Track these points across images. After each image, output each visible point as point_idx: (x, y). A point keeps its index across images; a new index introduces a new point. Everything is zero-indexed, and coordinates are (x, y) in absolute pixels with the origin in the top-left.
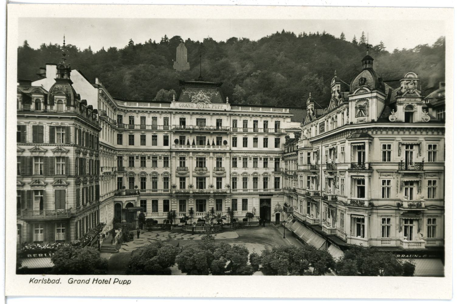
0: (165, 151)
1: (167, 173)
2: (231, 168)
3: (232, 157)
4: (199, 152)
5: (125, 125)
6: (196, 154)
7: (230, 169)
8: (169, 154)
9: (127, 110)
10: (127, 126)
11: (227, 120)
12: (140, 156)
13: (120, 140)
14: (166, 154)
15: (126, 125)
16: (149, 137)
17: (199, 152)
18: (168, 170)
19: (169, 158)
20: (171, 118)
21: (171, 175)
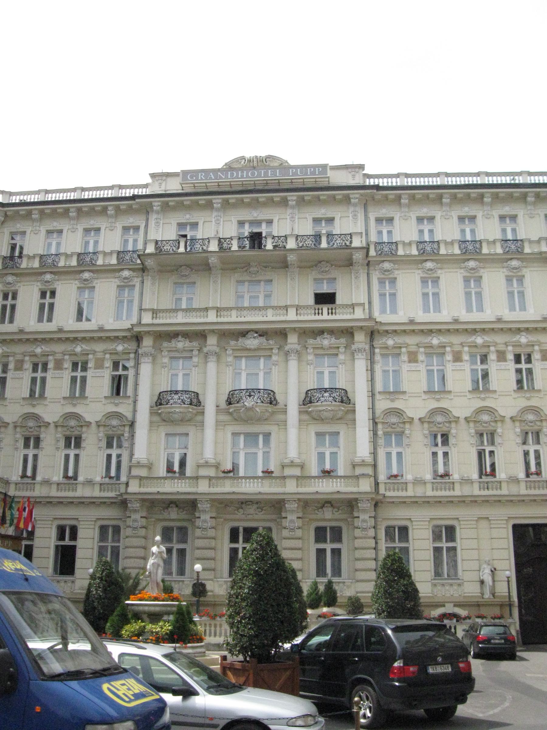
0: (117, 338)
1: (118, 415)
2: (378, 397)
3: (377, 351)
4: (244, 334)
6: (233, 343)
7: (373, 395)
8: (132, 346)
11: (355, 217)
14: (120, 348)
17: (244, 334)
18: (125, 409)
20: (146, 226)
21: (132, 424)
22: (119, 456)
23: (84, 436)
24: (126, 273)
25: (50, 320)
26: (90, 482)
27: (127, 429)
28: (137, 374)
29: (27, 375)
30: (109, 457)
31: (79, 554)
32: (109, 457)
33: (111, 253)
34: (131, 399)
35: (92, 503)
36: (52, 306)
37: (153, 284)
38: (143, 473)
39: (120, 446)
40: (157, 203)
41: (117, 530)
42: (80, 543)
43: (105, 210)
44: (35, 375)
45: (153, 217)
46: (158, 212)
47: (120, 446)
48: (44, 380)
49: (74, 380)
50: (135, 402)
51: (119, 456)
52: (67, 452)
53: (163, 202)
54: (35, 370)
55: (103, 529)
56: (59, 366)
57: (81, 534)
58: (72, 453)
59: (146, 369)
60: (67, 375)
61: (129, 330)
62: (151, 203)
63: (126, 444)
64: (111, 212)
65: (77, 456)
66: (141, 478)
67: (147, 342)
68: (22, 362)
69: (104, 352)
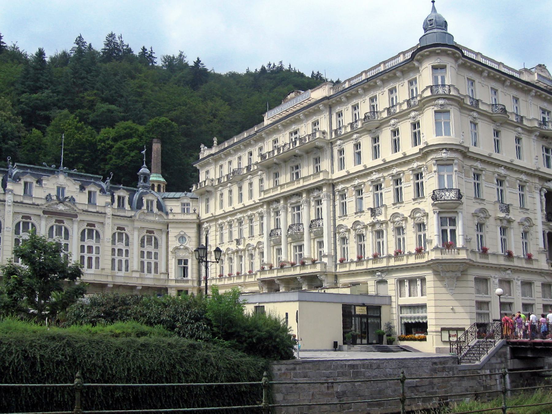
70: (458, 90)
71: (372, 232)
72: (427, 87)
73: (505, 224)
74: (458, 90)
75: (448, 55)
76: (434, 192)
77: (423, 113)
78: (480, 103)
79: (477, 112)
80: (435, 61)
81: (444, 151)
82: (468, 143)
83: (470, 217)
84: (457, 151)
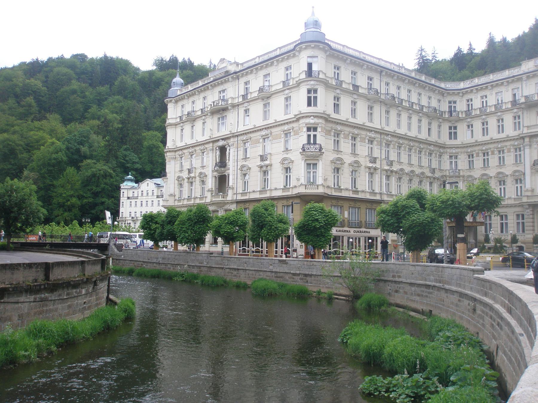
5: (460, 113)
8: (522, 141)
9: (463, 92)
10: (464, 113)
12: (480, 152)
13: (453, 135)
14: (516, 143)
15: (462, 112)
16: (492, 122)
18: (520, 168)
19: (522, 149)
21: (524, 174)
22: (521, 187)
23: (506, 180)
24: (515, 110)
25: (487, 134)
26: (510, 198)
27: (522, 176)
28: (524, 153)
29: (481, 158)
30: (517, 187)
31: (509, 225)
32: (517, 187)
33: (508, 102)
34: (523, 164)
35: (511, 206)
36: (487, 128)
37: (527, 114)
38: (529, 194)
39: (521, 183)
40: (524, 77)
41: (523, 215)
42: (509, 221)
43: (502, 83)
44: (484, 158)
45: (524, 83)
46: (526, 80)
47: (521, 183)
48: (488, 159)
49: (500, 158)
50: (525, 165)
51: (521, 187)
52: (500, 187)
53: (527, 76)
54: (484, 156)
55: (518, 216)
56: (493, 153)
57: (509, 217)
58: (502, 187)
59: (527, 151)
60: (496, 157)
61: (519, 136)
62: (522, 77)
63: (523, 182)
64: (505, 84)
65: (504, 188)
66: (528, 196)
67: (527, 140)
68: (478, 153)
69: (511, 145)
70: (325, 74)
71: (260, 172)
72: (303, 71)
73: (372, 170)
74: (325, 74)
75: (320, 49)
76: (303, 145)
77: (299, 90)
78: (343, 83)
79: (340, 89)
80: (309, 52)
81: (312, 118)
82: (330, 111)
83: (328, 163)
84: (321, 117)
